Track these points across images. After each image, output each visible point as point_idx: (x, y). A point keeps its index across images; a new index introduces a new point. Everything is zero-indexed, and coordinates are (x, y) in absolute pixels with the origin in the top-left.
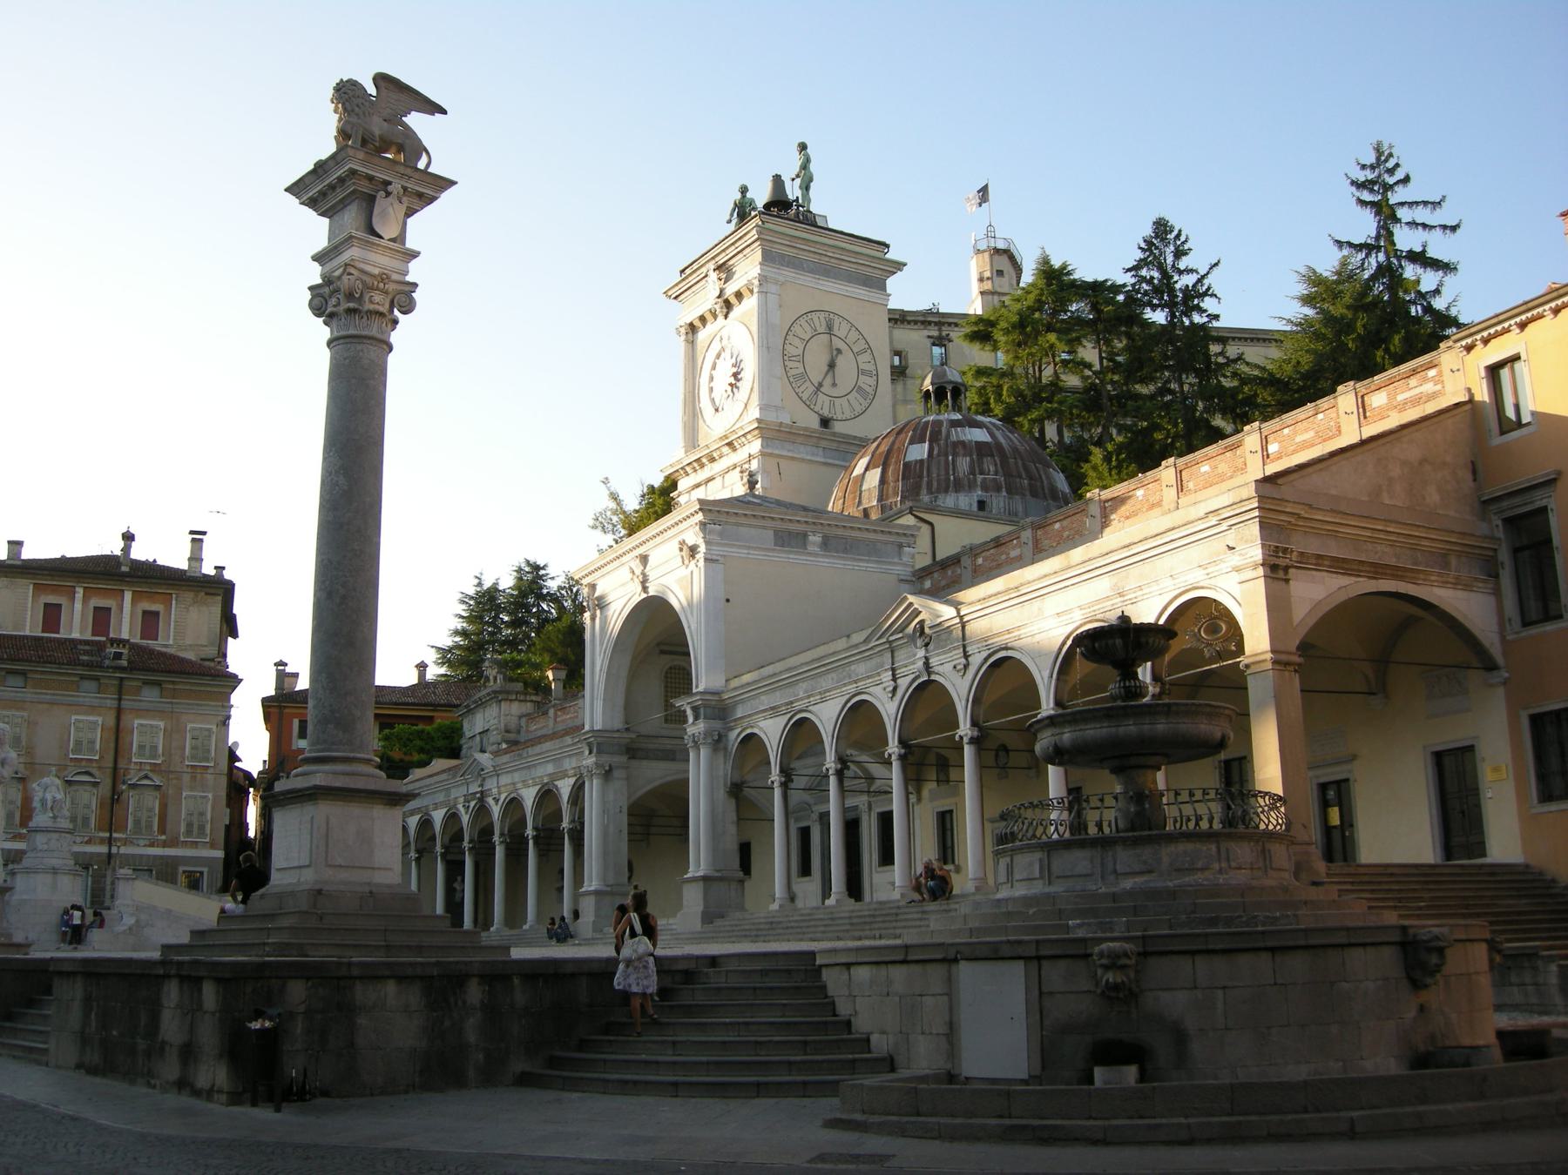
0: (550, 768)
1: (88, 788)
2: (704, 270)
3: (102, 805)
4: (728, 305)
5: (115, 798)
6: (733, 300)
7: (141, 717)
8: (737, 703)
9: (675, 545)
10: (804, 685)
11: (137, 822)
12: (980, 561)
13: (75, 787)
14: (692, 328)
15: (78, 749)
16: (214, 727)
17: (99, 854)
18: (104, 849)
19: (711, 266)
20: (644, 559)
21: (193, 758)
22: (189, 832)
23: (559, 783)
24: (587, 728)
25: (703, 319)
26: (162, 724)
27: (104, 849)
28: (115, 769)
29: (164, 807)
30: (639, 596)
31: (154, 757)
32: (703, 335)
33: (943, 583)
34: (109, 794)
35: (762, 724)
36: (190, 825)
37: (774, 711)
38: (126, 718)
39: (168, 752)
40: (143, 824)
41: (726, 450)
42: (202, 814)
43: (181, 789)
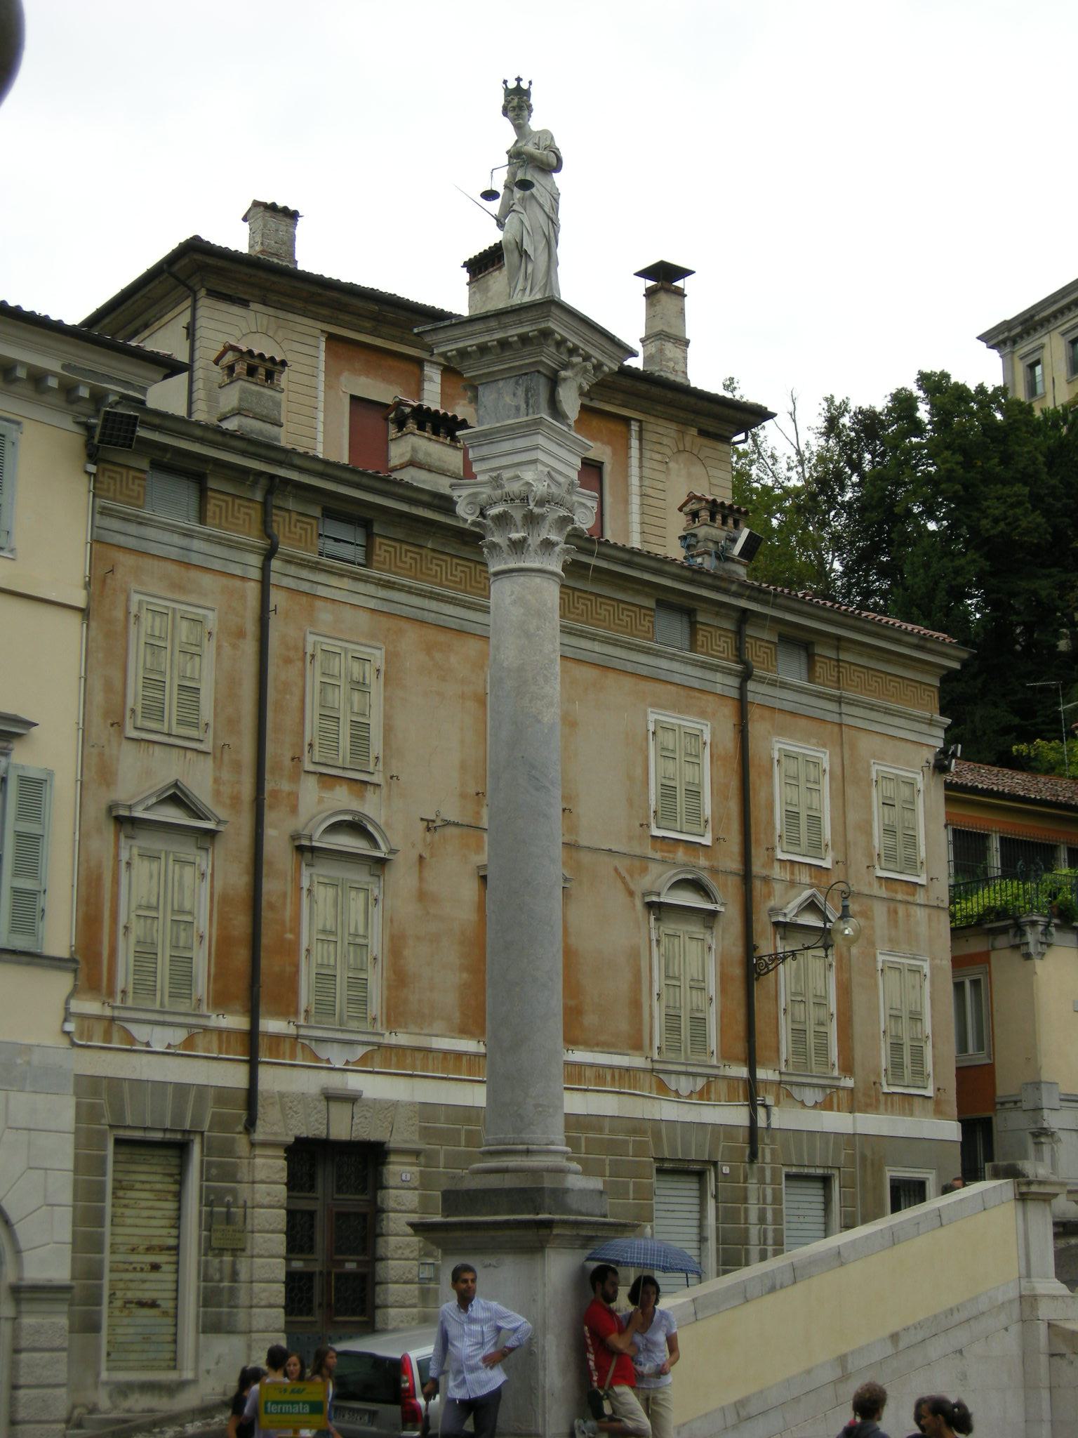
1: (696, 929)
3: (724, 979)
5: (753, 969)
7: (782, 731)
11: (799, 1034)
13: (669, 927)
15: (666, 814)
16: (919, 778)
17: (729, 1130)
18: (737, 1116)
21: (891, 857)
22: (897, 1066)
26: (825, 758)
27: (737, 1116)
28: (747, 876)
29: (845, 991)
31: (817, 847)
34: (737, 951)
36: (896, 1047)
38: (757, 728)
39: (843, 843)
40: (811, 1041)
42: (916, 1018)
43: (872, 944)
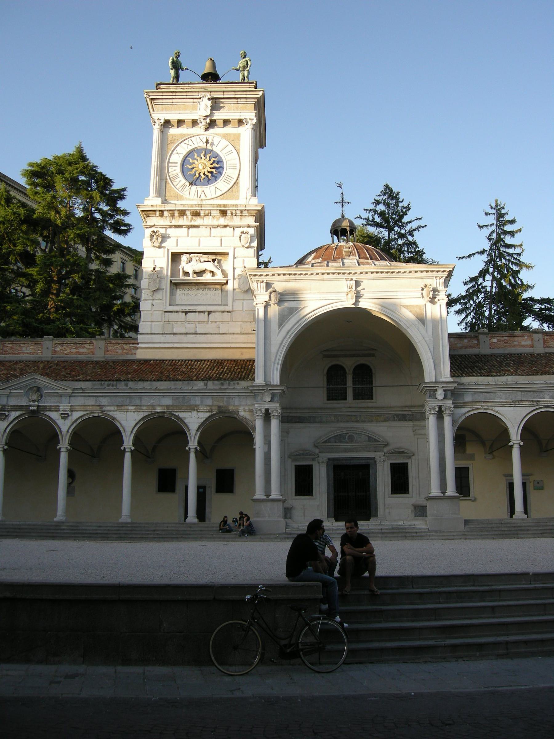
0: (168, 402)
2: (201, 95)
4: (212, 124)
6: (220, 123)
8: (467, 392)
9: (421, 283)
10: (551, 394)
12: (495, 340)
14: (167, 123)
19: (208, 95)
20: (358, 283)
23: (182, 415)
24: (259, 379)
25: (180, 123)
30: (349, 303)
32: (173, 131)
33: (460, 345)
35: (497, 409)
37: (515, 404)
41: (217, 213)
